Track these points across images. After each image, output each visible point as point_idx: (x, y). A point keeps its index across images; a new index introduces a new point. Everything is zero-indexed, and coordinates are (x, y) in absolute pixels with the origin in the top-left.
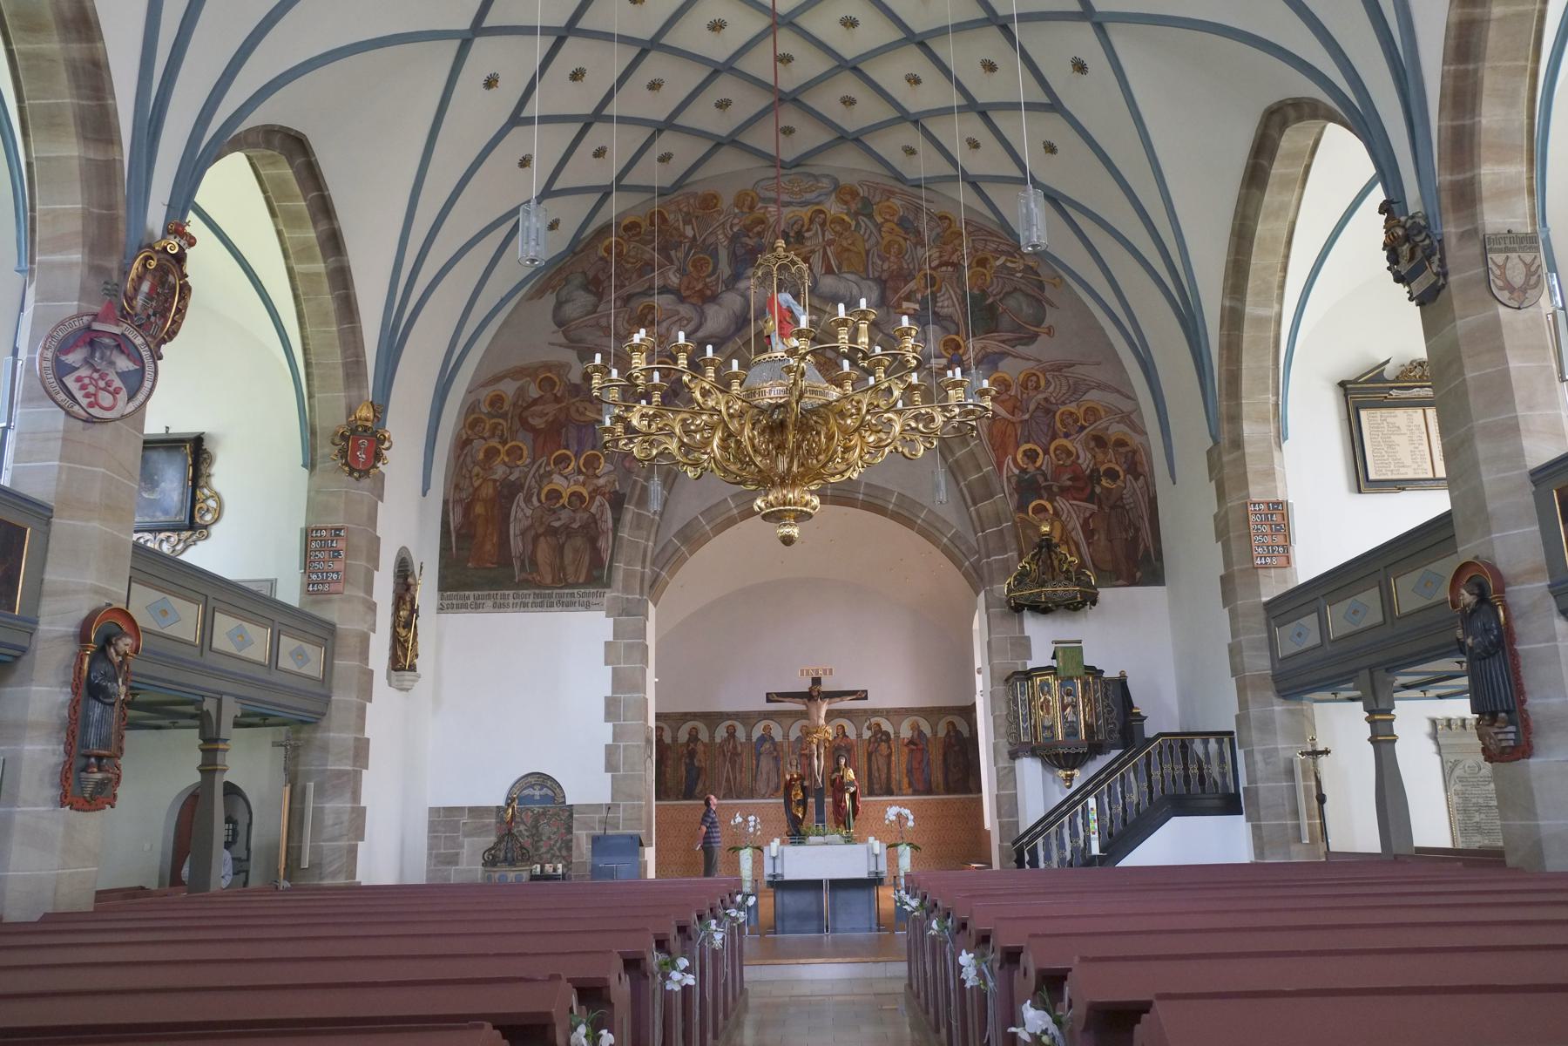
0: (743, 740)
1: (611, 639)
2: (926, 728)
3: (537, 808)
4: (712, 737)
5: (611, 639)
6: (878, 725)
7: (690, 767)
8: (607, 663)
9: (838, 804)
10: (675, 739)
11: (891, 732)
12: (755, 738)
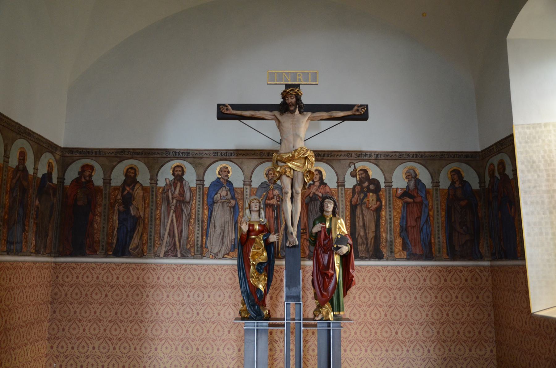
0: (193, 185)
2: (425, 177)
4: (154, 179)
6: (365, 171)
7: (125, 215)
10: (107, 180)
11: (381, 180)
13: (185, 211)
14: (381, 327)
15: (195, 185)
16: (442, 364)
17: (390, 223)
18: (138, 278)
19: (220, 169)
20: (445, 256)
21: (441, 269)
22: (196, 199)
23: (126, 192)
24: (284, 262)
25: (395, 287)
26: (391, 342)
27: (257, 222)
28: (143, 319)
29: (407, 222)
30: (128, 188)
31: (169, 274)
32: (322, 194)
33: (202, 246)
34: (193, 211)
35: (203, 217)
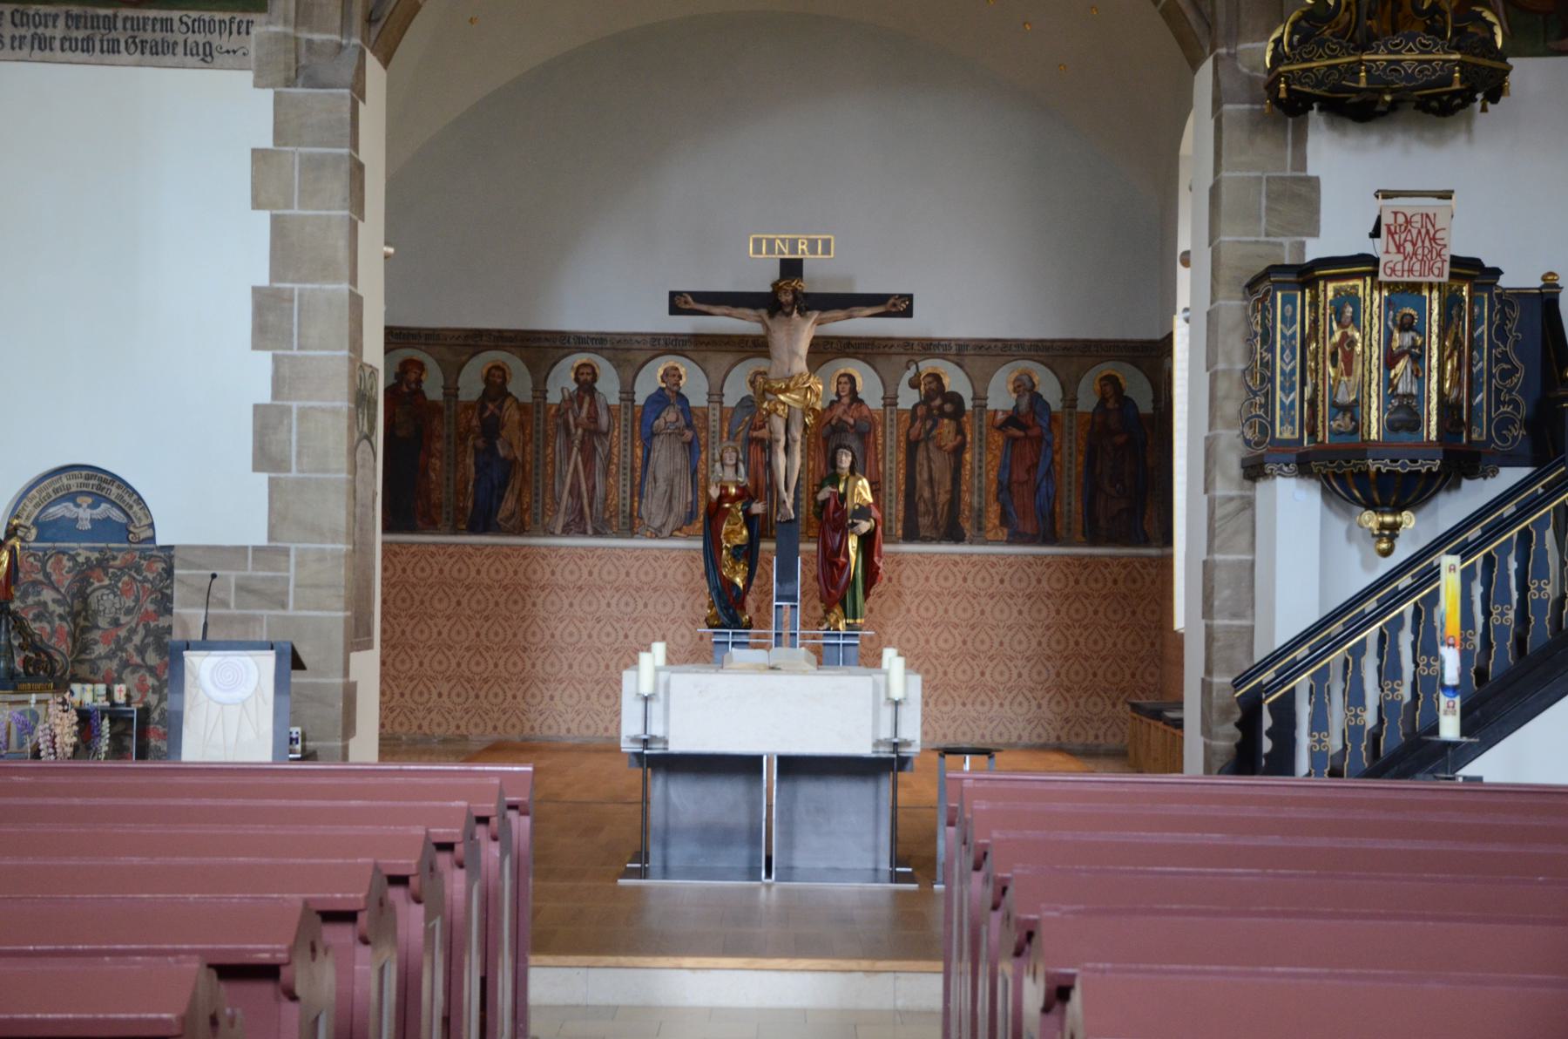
0: (614, 400)
1: (267, 142)
2: (1049, 388)
3: (84, 551)
4: (540, 390)
5: (267, 142)
6: (937, 378)
7: (486, 455)
8: (257, 204)
9: (831, 560)
10: (451, 391)
12: (642, 394)
13: (600, 449)
14: (954, 664)
15: (617, 402)
16: (1062, 728)
17: (980, 475)
18: (516, 573)
19: (665, 370)
20: (1079, 537)
21: (1070, 561)
22: (619, 427)
23: (487, 414)
24: (772, 546)
25: (982, 593)
26: (973, 689)
27: (732, 482)
28: (527, 646)
29: (1011, 474)
30: (491, 406)
31: (572, 566)
32: (855, 421)
33: (631, 515)
34: (615, 450)
35: (633, 462)
